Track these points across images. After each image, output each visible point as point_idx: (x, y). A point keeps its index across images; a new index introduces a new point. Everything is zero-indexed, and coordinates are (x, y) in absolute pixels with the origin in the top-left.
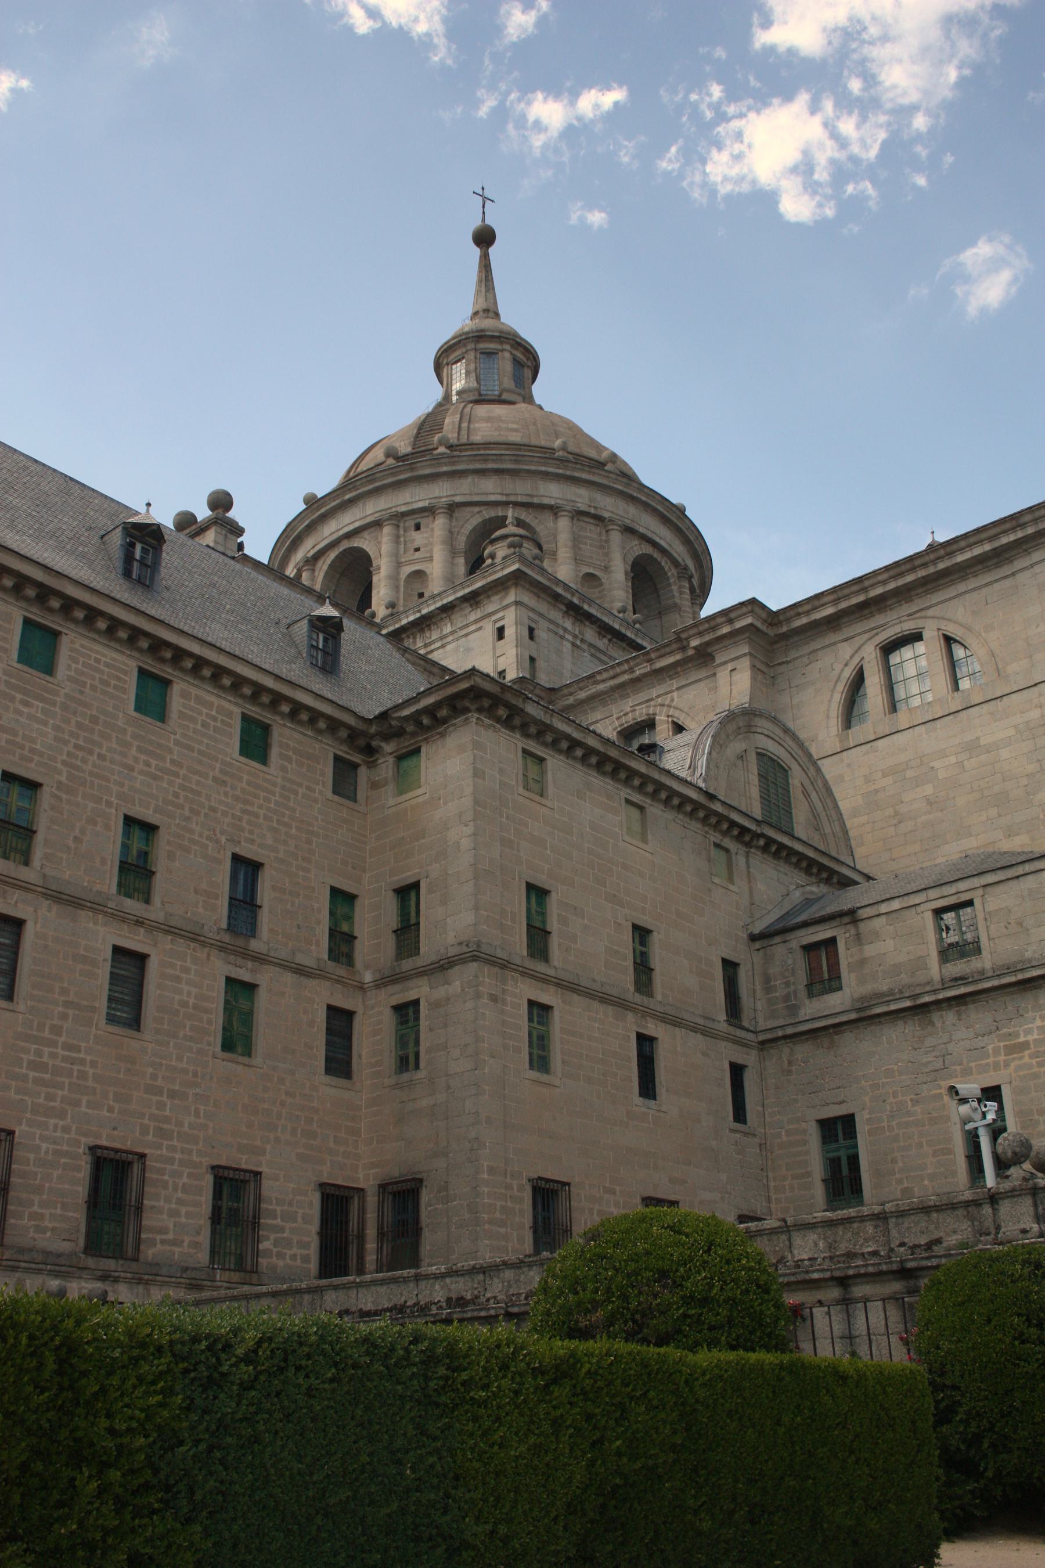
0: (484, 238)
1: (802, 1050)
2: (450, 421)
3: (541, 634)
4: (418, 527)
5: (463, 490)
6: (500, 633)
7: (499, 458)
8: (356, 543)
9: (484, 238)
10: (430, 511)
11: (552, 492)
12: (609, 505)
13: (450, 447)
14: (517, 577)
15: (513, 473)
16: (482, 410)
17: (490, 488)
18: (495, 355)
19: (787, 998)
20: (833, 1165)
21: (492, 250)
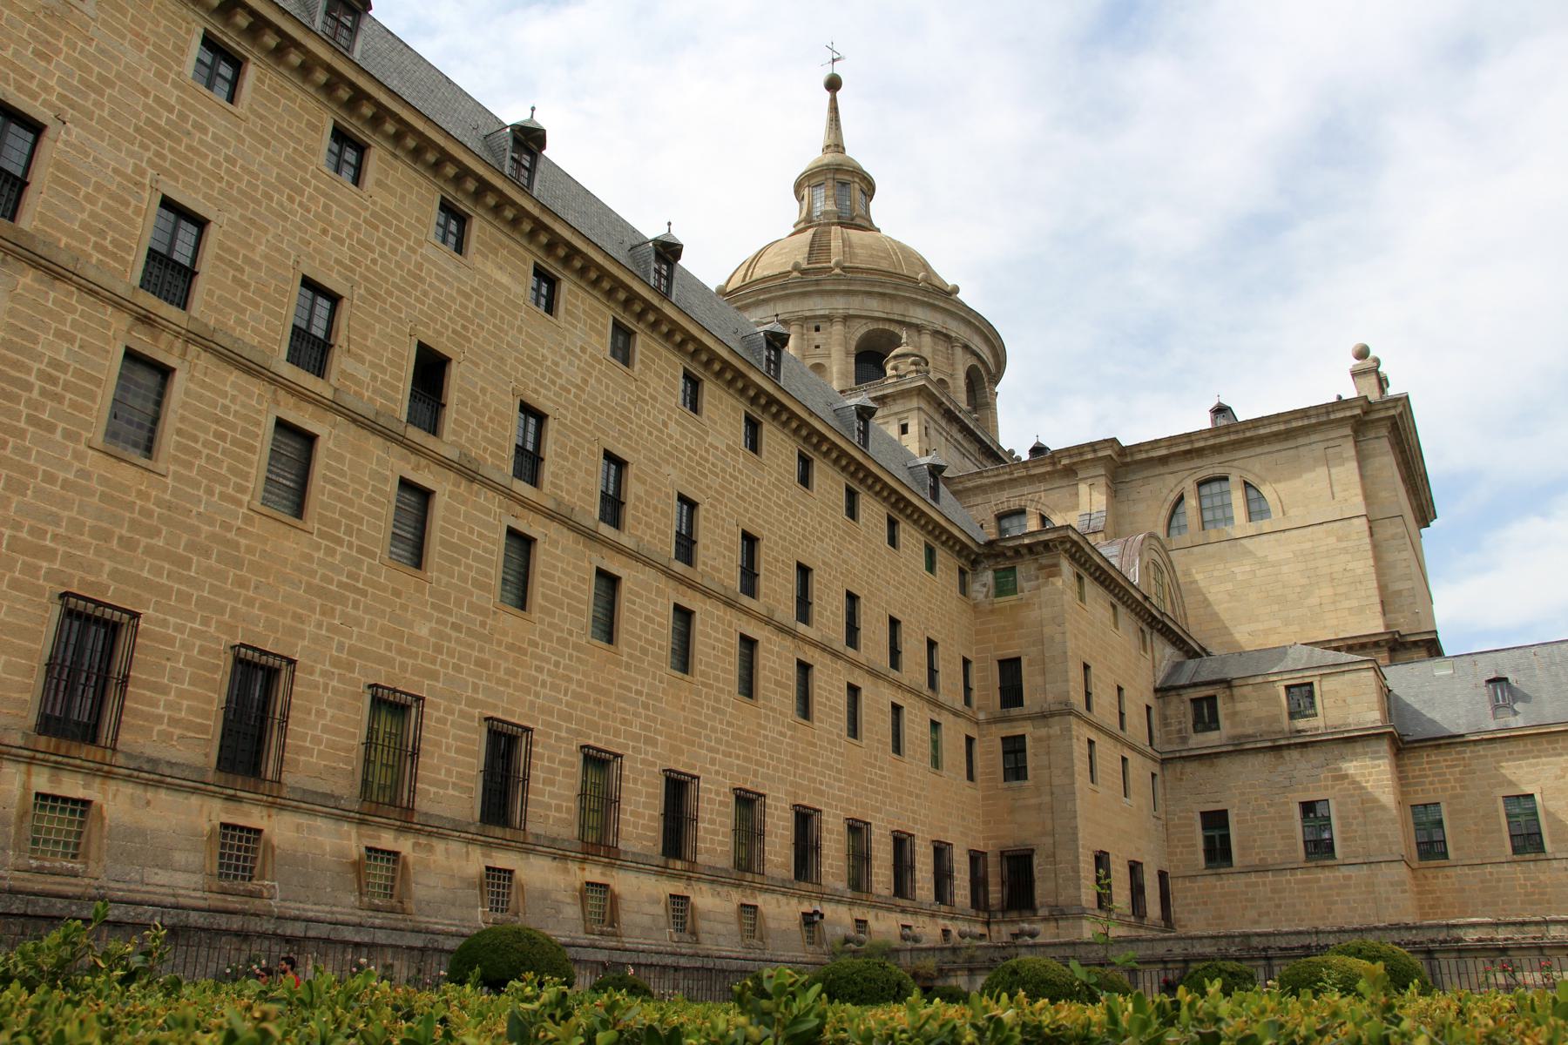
0: (833, 84)
1: (1191, 767)
2: (836, 244)
3: (932, 432)
4: (817, 329)
5: (855, 305)
7: (882, 284)
9: (833, 84)
10: (829, 319)
11: (919, 315)
13: (843, 268)
14: (921, 391)
15: (892, 297)
16: (854, 234)
17: (875, 307)
18: (840, 185)
19: (1180, 731)
20: (1208, 841)
21: (838, 94)
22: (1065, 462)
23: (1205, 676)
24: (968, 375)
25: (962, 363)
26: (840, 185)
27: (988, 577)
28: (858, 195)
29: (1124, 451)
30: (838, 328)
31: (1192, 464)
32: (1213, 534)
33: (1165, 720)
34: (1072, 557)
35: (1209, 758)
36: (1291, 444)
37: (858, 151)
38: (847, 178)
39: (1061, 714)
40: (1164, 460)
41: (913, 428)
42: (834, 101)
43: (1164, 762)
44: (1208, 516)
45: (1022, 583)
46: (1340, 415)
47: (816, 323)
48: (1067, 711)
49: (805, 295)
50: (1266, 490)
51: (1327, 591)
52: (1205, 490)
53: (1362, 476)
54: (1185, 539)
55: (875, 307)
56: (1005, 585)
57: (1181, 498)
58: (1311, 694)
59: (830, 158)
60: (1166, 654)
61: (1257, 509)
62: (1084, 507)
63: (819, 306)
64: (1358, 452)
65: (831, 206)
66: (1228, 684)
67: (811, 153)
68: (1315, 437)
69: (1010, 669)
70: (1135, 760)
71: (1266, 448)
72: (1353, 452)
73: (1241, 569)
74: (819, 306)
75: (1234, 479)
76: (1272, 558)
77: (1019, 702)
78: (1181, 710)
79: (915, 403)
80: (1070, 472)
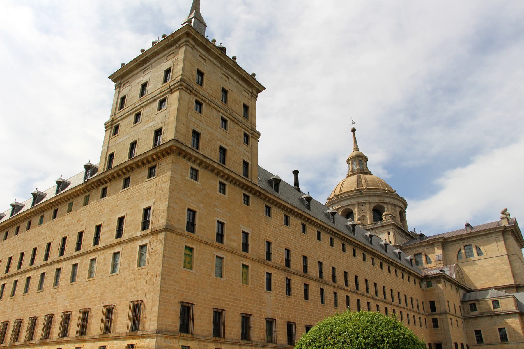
0: (354, 130)
1: (471, 320)
5: (371, 199)
6: (389, 234)
8: (349, 207)
9: (354, 130)
10: (365, 203)
11: (387, 200)
12: (396, 202)
14: (393, 224)
15: (380, 196)
17: (376, 199)
22: (431, 242)
23: (472, 298)
24: (400, 214)
25: (398, 210)
26: (359, 161)
27: (425, 283)
28: (364, 163)
29: (445, 239)
30: (368, 206)
31: (462, 242)
32: (469, 259)
33: (463, 309)
34: (443, 278)
35: (475, 318)
36: (487, 237)
37: (362, 150)
38: (361, 158)
39: (445, 313)
40: (455, 241)
41: (391, 233)
42: (354, 135)
43: (464, 319)
44: (467, 254)
45: (433, 284)
46: (499, 230)
47: (362, 204)
48: (446, 313)
49: (358, 197)
50: (481, 248)
51: (499, 273)
52: (466, 248)
53: (505, 244)
54: (462, 260)
55: (376, 199)
56: (429, 285)
57: (460, 250)
58: (498, 303)
59: (356, 153)
60: (462, 292)
61: (479, 253)
62: (436, 254)
63: (362, 200)
64: (504, 238)
65: (358, 167)
66: (478, 300)
67: (350, 153)
68: (493, 235)
69: (432, 303)
70: (459, 320)
71: (481, 238)
72: (502, 239)
73: (477, 268)
74: (362, 200)
75: (473, 245)
76: (484, 265)
77: (435, 311)
78: (467, 307)
79: (391, 227)
80: (432, 244)
